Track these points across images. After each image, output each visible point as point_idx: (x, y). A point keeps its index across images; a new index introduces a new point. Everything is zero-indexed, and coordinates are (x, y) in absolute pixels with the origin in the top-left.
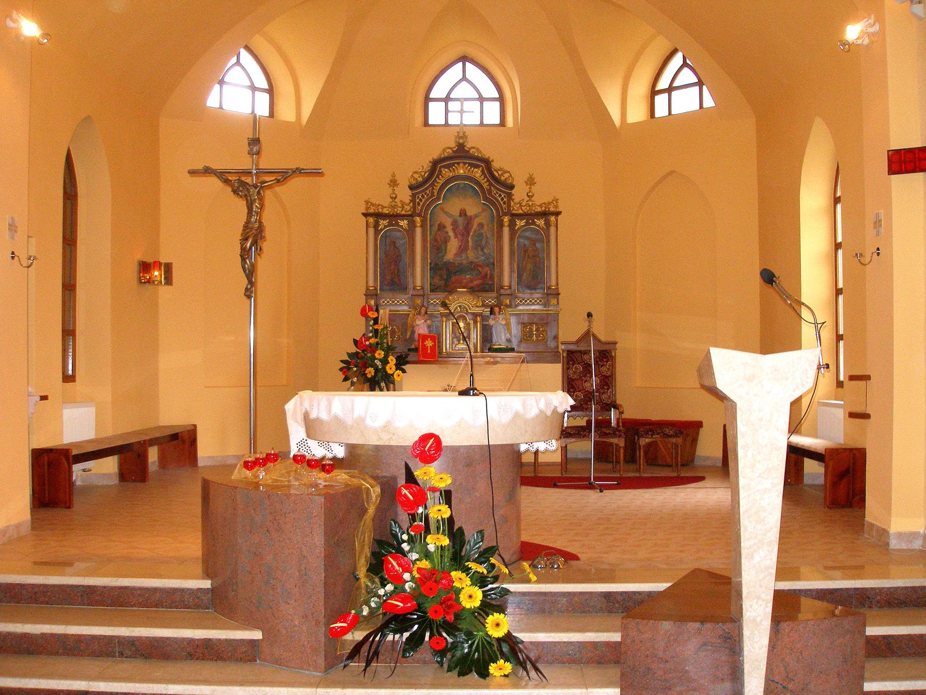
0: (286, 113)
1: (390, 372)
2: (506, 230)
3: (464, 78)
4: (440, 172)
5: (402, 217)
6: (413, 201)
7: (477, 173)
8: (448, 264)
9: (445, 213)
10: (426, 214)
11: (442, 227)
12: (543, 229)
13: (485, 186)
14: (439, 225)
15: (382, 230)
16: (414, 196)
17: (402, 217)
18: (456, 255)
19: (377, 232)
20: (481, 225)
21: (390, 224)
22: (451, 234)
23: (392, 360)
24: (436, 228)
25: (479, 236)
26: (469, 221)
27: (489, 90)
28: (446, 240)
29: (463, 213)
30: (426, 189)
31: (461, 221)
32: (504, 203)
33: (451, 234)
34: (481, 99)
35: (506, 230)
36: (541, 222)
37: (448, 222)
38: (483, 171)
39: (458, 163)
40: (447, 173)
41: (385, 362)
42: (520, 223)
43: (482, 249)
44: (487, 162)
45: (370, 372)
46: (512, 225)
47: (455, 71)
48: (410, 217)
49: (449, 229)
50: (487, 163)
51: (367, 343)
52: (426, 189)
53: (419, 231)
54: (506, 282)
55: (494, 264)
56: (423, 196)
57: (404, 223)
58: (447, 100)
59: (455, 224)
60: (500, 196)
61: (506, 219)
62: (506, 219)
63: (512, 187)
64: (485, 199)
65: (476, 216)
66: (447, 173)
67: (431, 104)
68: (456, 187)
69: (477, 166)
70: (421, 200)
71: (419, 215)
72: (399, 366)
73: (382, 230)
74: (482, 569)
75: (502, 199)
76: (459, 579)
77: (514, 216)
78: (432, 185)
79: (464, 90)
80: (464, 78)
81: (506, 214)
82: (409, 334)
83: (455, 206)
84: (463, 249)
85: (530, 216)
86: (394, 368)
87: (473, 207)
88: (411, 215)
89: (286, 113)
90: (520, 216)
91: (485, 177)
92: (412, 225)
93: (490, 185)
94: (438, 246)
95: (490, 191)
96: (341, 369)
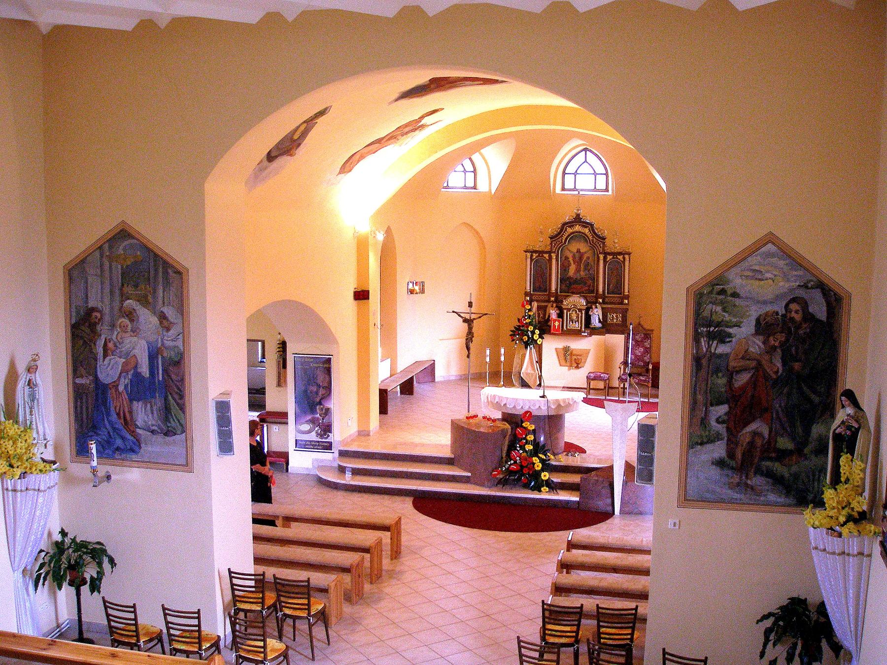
0: (483, 187)
1: (534, 337)
2: (601, 262)
3: (586, 161)
4: (566, 229)
5: (546, 252)
6: (551, 244)
7: (586, 231)
8: (570, 278)
9: (569, 251)
10: (558, 251)
11: (567, 258)
12: (621, 261)
13: (591, 238)
14: (566, 257)
15: (534, 259)
16: (552, 242)
17: (546, 252)
18: (575, 273)
19: (532, 260)
20: (588, 258)
21: (539, 256)
22: (572, 262)
23: (537, 332)
24: (563, 258)
25: (587, 265)
26: (581, 255)
27: (600, 169)
28: (569, 265)
29: (578, 251)
30: (559, 238)
31: (577, 255)
32: (601, 247)
33: (572, 262)
34: (595, 174)
35: (601, 262)
36: (621, 257)
37: (570, 255)
38: (589, 229)
39: (576, 225)
40: (570, 230)
41: (533, 333)
42: (609, 257)
43: (589, 271)
44: (592, 225)
45: (525, 338)
46: (605, 258)
47: (581, 157)
48: (549, 253)
49: (571, 259)
50: (590, 226)
51: (524, 322)
52: (559, 238)
53: (554, 262)
54: (601, 290)
55: (595, 279)
56: (557, 243)
57: (546, 256)
58: (575, 174)
59: (574, 257)
60: (598, 243)
61: (601, 257)
62: (601, 257)
63: (604, 239)
64: (590, 244)
65: (585, 253)
66: (570, 230)
67: (566, 175)
68: (574, 237)
69: (586, 227)
70: (555, 244)
71: (554, 252)
72: (541, 336)
73: (534, 259)
74: (544, 457)
75: (599, 245)
76: (535, 460)
77: (606, 254)
78: (562, 236)
79: (585, 168)
80: (586, 161)
81: (601, 253)
82: (547, 317)
83: (574, 247)
84: (578, 270)
85: (615, 254)
86: (538, 336)
87: (583, 247)
88: (550, 252)
89: (483, 187)
90: (610, 254)
91: (591, 233)
92: (550, 257)
93: (593, 237)
94: (565, 268)
95: (593, 240)
96: (511, 335)
